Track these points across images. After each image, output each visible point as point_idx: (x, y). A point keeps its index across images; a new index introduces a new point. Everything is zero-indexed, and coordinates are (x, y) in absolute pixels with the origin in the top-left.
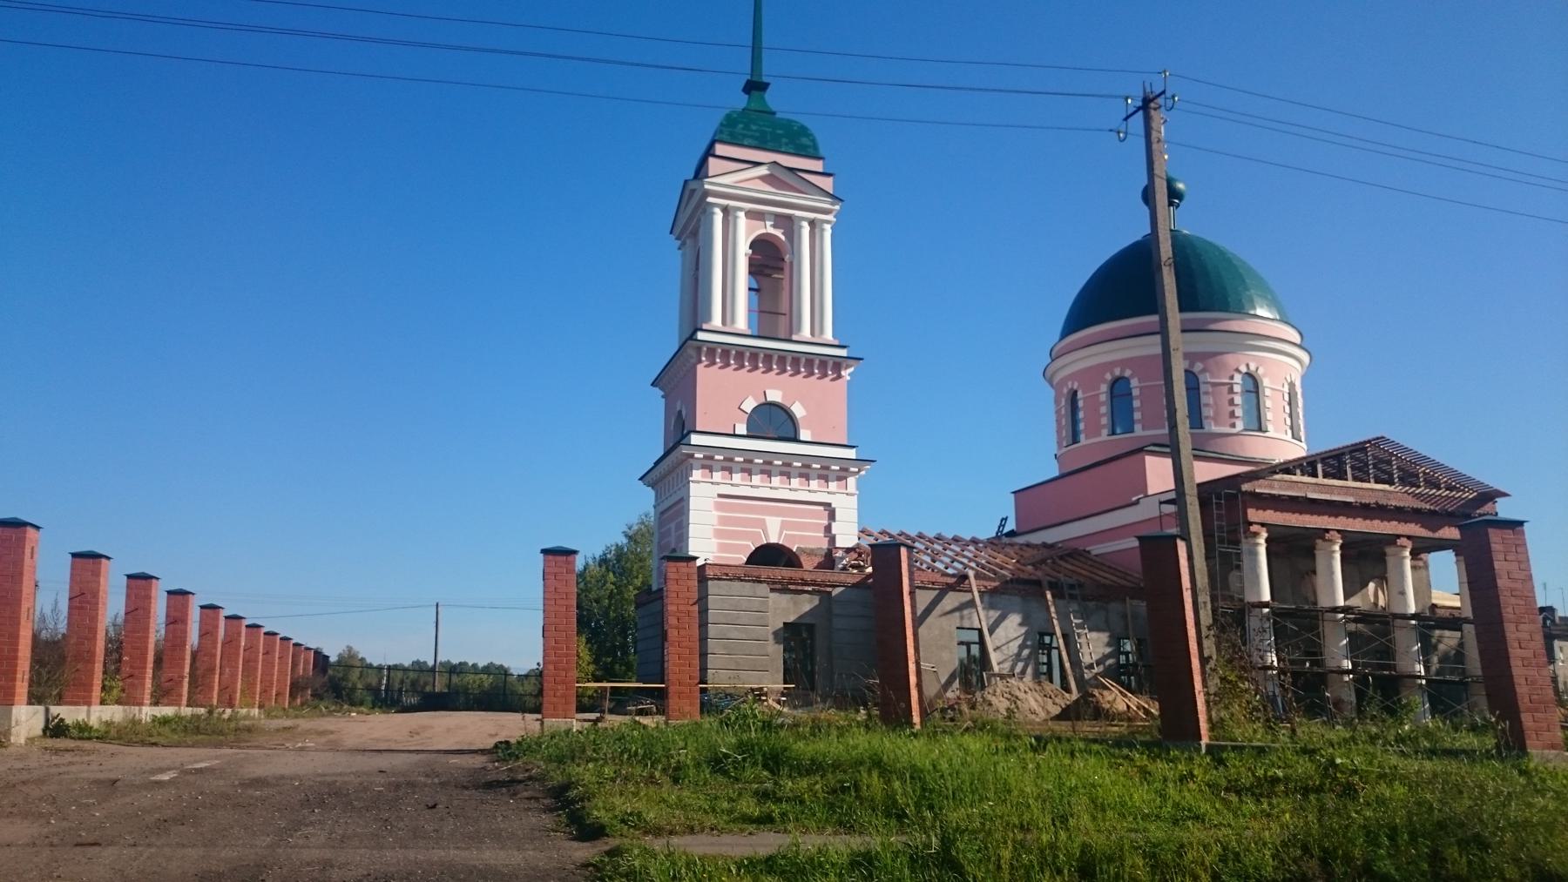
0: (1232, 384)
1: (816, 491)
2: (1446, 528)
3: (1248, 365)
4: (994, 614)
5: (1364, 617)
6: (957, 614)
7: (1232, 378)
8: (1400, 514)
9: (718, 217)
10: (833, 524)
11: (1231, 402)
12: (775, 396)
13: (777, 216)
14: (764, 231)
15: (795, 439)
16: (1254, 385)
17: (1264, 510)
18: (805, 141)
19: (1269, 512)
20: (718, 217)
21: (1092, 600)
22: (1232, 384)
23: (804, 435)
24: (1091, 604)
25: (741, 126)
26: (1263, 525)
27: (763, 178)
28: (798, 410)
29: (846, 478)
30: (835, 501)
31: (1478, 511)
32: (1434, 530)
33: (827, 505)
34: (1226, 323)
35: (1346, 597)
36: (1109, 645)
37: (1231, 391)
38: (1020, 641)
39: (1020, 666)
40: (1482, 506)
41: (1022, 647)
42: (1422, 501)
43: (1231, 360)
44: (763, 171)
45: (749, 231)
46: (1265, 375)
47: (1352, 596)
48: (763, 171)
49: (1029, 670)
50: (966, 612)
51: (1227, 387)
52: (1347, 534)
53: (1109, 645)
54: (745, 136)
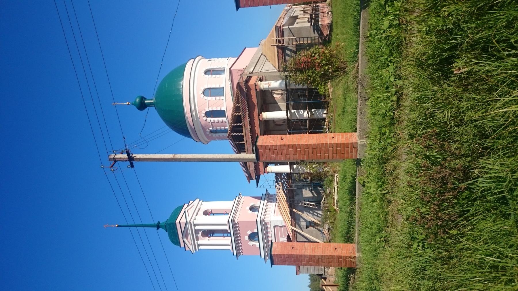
0: (211, 122)
1: (271, 230)
2: (253, 100)
3: (203, 117)
4: (301, 220)
5: (288, 99)
6: (303, 229)
7: (209, 122)
8: (252, 124)
9: (201, 247)
10: (279, 226)
11: (218, 122)
12: (247, 238)
13: (196, 233)
14: (201, 236)
15: (258, 233)
16: (209, 114)
17: (260, 169)
18: (172, 225)
19: (256, 129)
20: (201, 247)
21: (293, 193)
22: (211, 122)
23: (256, 231)
24: (295, 193)
25: (174, 240)
26: (264, 169)
27: (187, 238)
28: (249, 232)
29: (266, 223)
30: (273, 226)
31: (245, 90)
32: (255, 106)
33: (274, 227)
34: (191, 125)
35: (280, 110)
36: (306, 189)
37: (214, 122)
38: (308, 213)
39: (315, 213)
40: (242, 88)
41: (310, 213)
42: (246, 115)
43: (203, 123)
44: (185, 240)
45: (202, 239)
46: (204, 110)
47: (280, 108)
48: (185, 240)
49: (316, 211)
50: (302, 227)
51: (213, 124)
52: (259, 113)
53: (306, 189)
54: (176, 240)
